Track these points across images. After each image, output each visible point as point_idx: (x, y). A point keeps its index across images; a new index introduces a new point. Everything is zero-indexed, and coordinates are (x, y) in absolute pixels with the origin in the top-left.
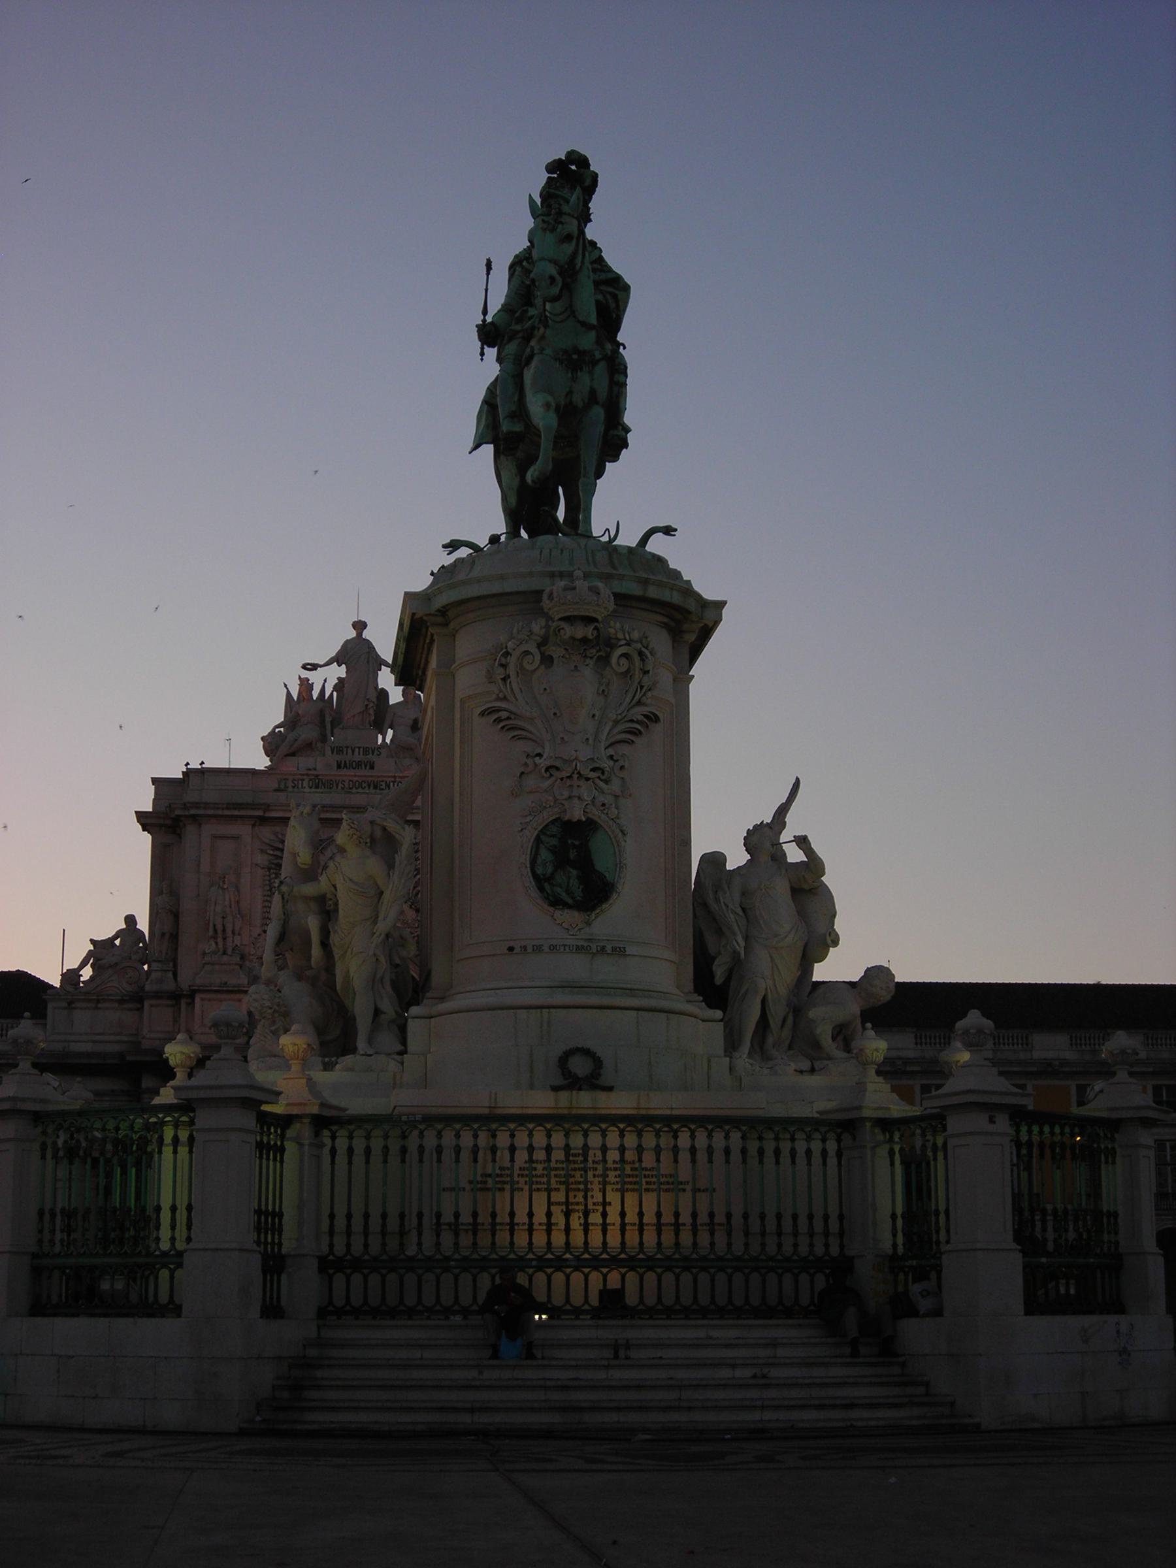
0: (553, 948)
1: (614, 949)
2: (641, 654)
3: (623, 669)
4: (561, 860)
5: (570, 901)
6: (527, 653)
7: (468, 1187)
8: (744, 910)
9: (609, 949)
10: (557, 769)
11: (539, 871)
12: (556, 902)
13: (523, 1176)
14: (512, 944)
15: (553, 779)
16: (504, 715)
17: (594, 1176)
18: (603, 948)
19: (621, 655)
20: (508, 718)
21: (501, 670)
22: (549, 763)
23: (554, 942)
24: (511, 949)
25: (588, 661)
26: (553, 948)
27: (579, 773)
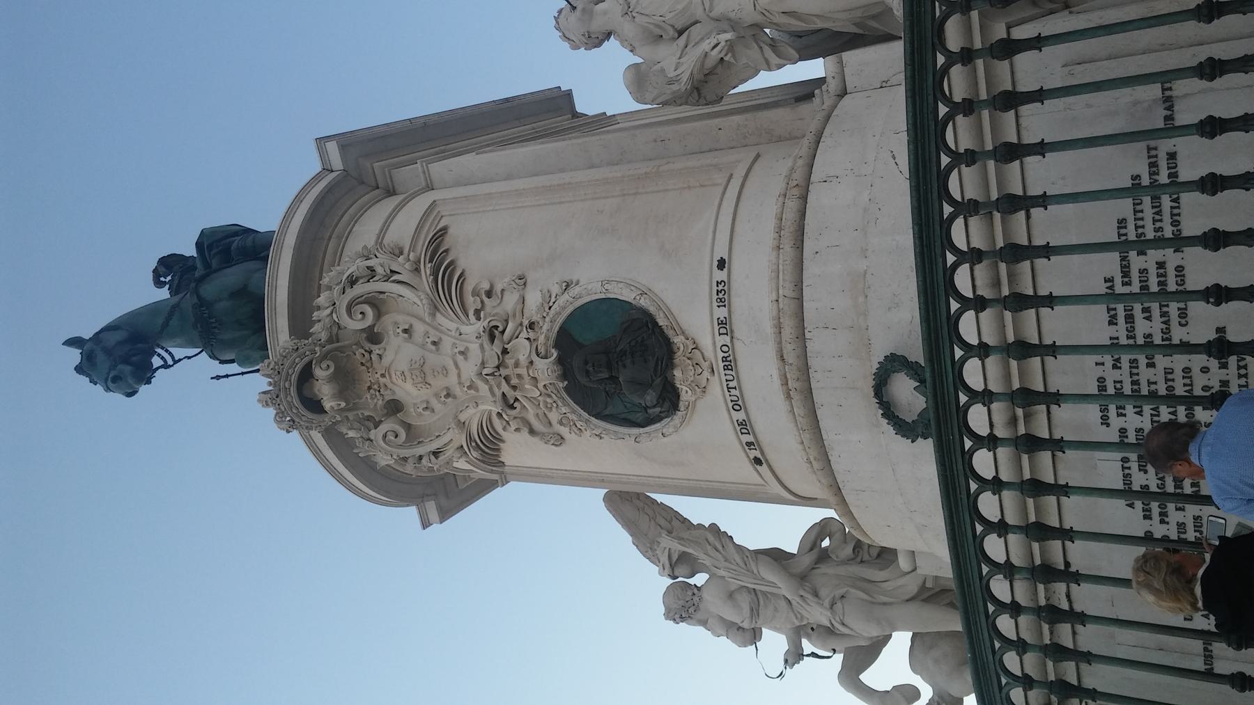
0: (737, 405)
1: (722, 302)
2: (352, 281)
3: (368, 310)
8: (680, 33)
9: (722, 313)
13: (1163, 514)
17: (1151, 365)
18: (722, 323)
19: (350, 316)
21: (424, 461)
23: (730, 405)
25: (374, 357)
26: (737, 405)
27: (498, 367)
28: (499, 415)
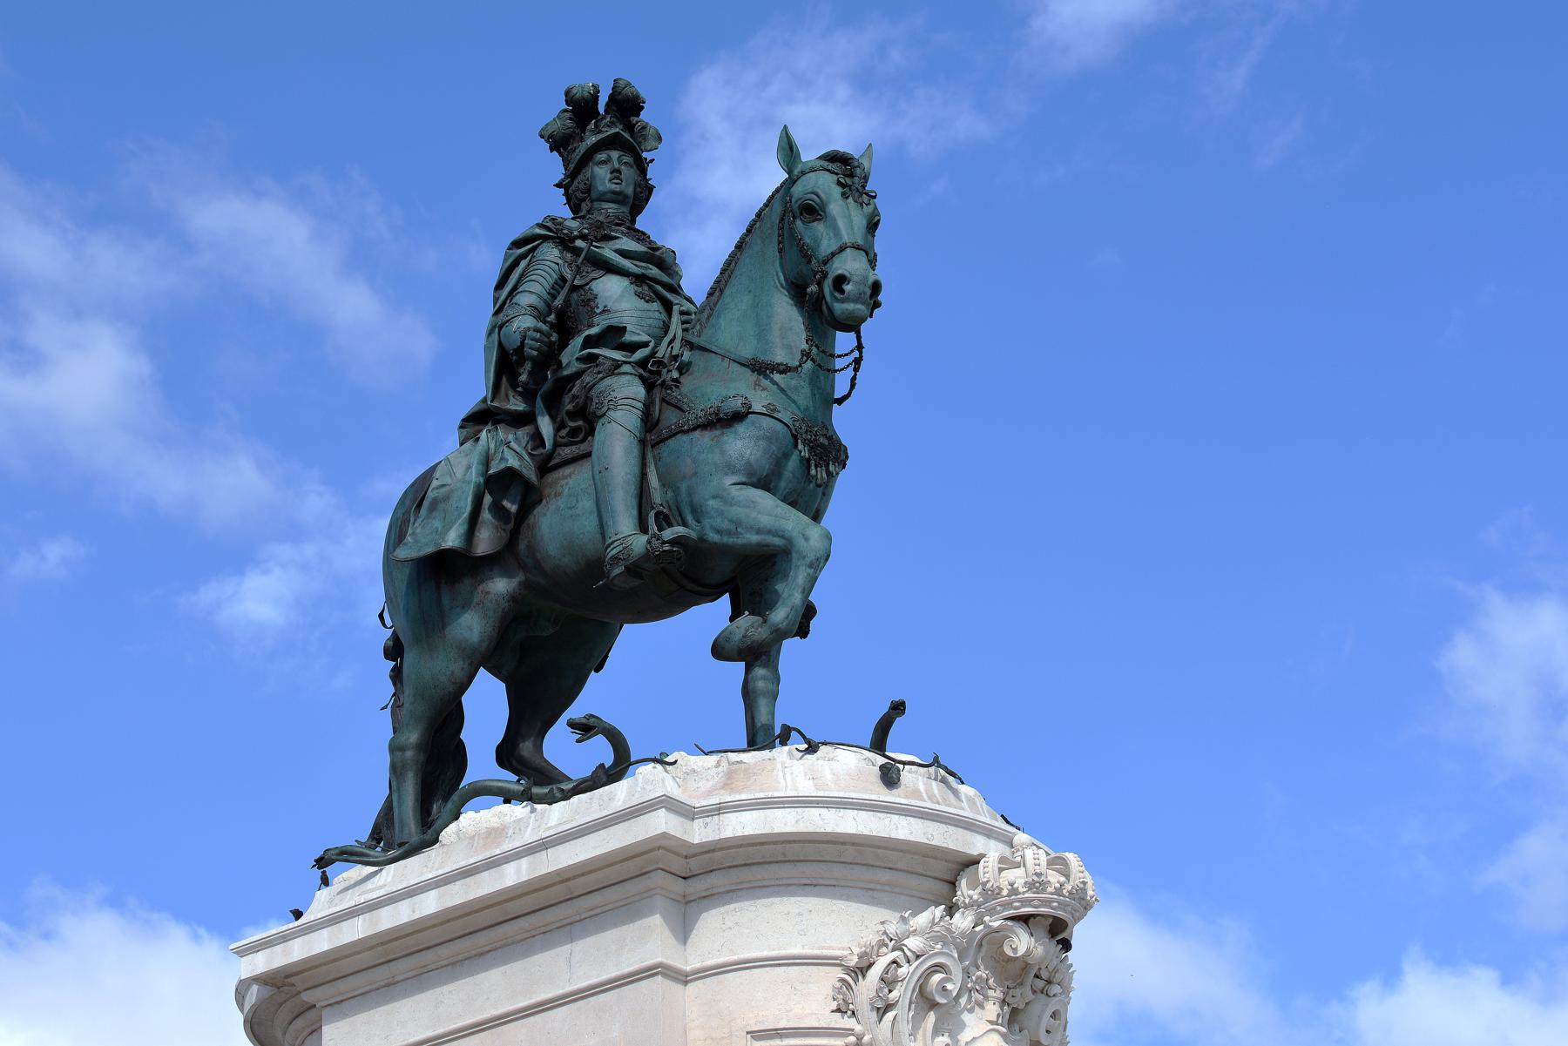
6: (939, 968)
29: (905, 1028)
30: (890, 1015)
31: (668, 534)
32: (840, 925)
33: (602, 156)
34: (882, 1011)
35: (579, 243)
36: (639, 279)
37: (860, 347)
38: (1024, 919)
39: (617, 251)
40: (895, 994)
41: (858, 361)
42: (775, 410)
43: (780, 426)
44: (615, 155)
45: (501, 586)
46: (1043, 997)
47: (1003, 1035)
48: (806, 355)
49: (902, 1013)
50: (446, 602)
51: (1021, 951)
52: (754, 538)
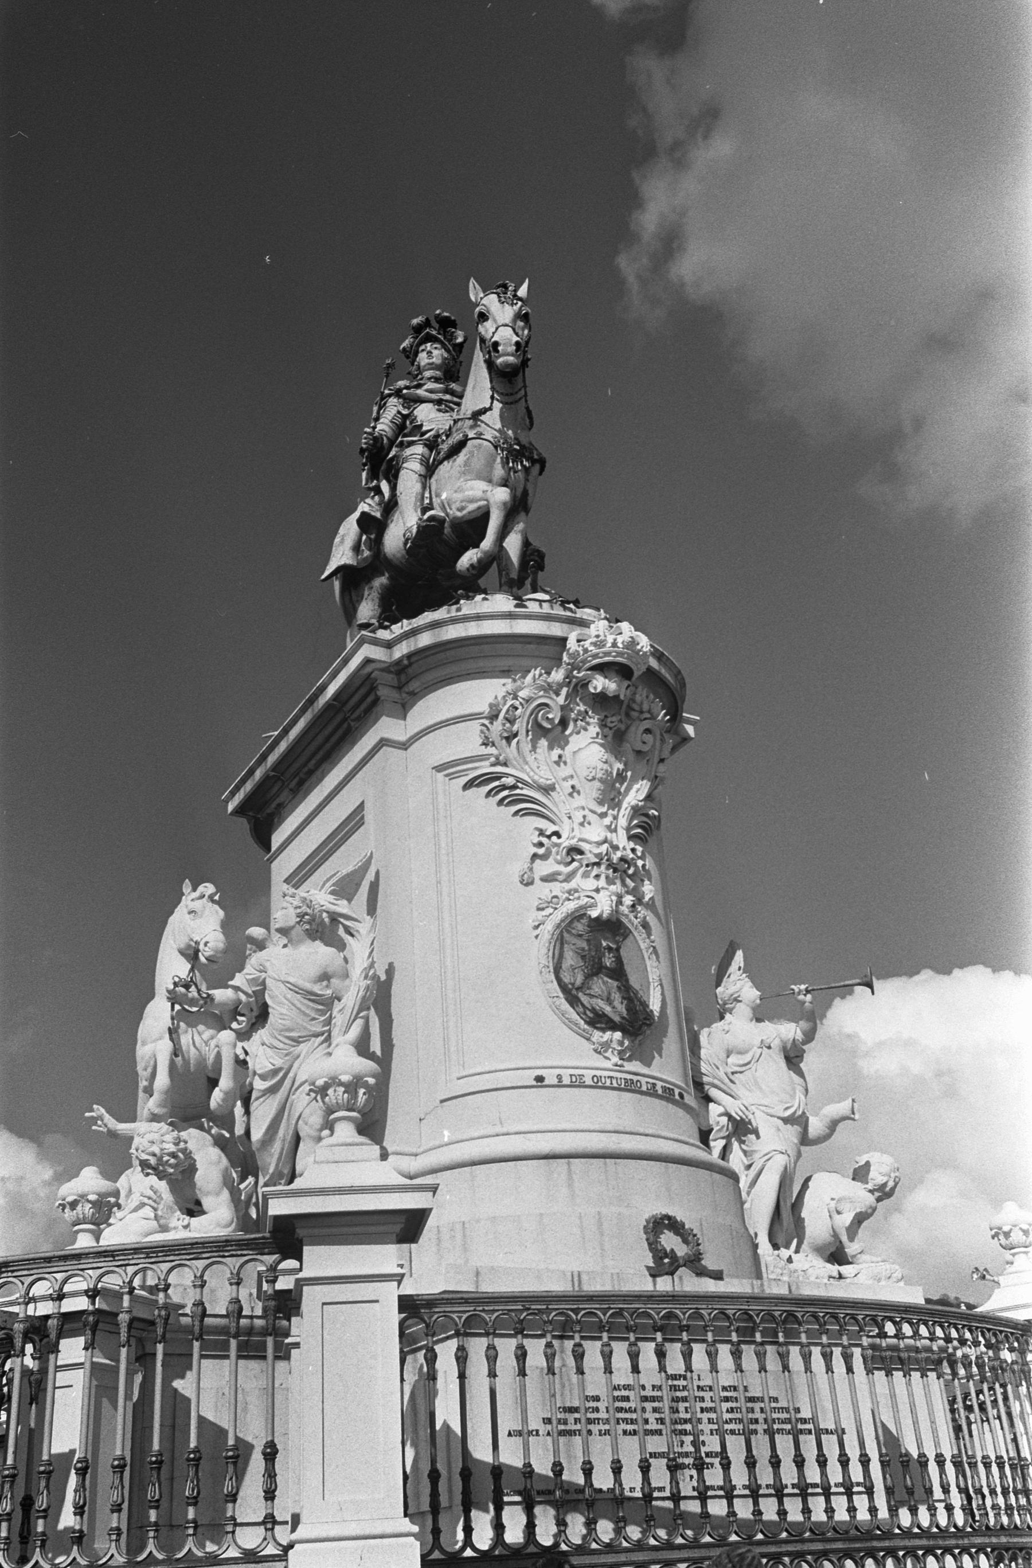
4: (595, 969)
5: (617, 1019)
7: (543, 1429)
10: (581, 852)
11: (567, 979)
12: (598, 1020)
14: (539, 1072)
15: (575, 864)
16: (510, 781)
20: (514, 787)
22: (573, 842)
23: (598, 1073)
24: (540, 1079)
28: (557, 834)
29: (526, 747)
30: (516, 740)
31: (425, 517)
32: (480, 693)
33: (422, 347)
34: (508, 739)
35: (405, 391)
36: (439, 402)
37: (525, 387)
38: (601, 668)
39: (427, 391)
40: (515, 728)
41: (526, 395)
42: (481, 434)
43: (486, 443)
44: (429, 344)
45: (381, 581)
46: (638, 722)
47: (602, 745)
48: (492, 398)
49: (524, 740)
50: (354, 598)
51: (598, 690)
52: (472, 507)
